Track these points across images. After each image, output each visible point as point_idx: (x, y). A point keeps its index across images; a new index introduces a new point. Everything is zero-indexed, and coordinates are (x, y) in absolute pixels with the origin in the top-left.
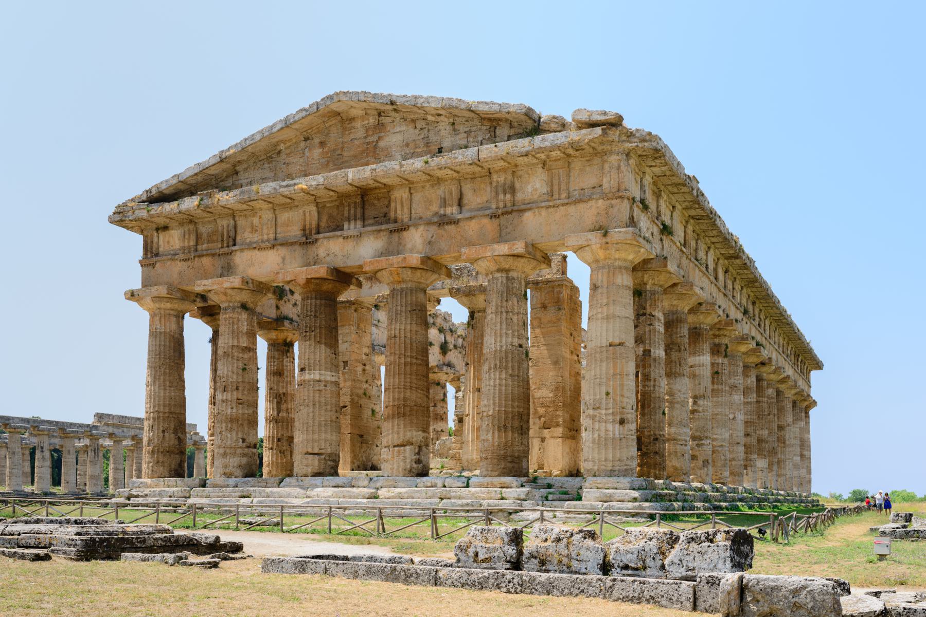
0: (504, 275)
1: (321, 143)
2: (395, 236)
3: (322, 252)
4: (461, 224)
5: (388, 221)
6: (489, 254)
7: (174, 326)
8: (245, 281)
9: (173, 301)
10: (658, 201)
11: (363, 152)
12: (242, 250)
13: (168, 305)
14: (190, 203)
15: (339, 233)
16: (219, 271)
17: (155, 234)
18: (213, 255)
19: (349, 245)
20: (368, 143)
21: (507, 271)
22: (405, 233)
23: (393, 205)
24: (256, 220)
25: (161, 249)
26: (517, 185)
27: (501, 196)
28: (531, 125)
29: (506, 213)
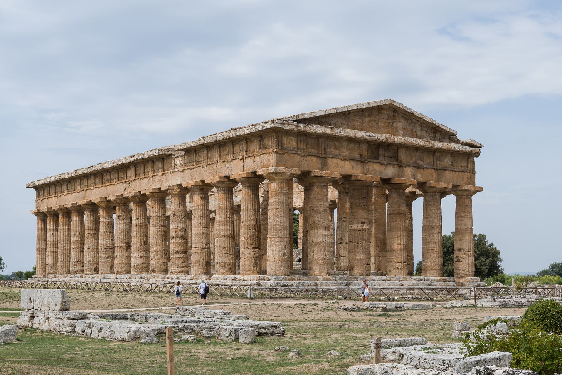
2: (401, 168)
3: (371, 169)
4: (425, 169)
5: (397, 161)
11: (387, 126)
12: (332, 158)
14: (320, 129)
16: (320, 166)
18: (317, 156)
19: (382, 168)
20: (389, 123)
22: (405, 168)
24: (337, 144)
27: (438, 162)
28: (450, 136)
29: (441, 169)
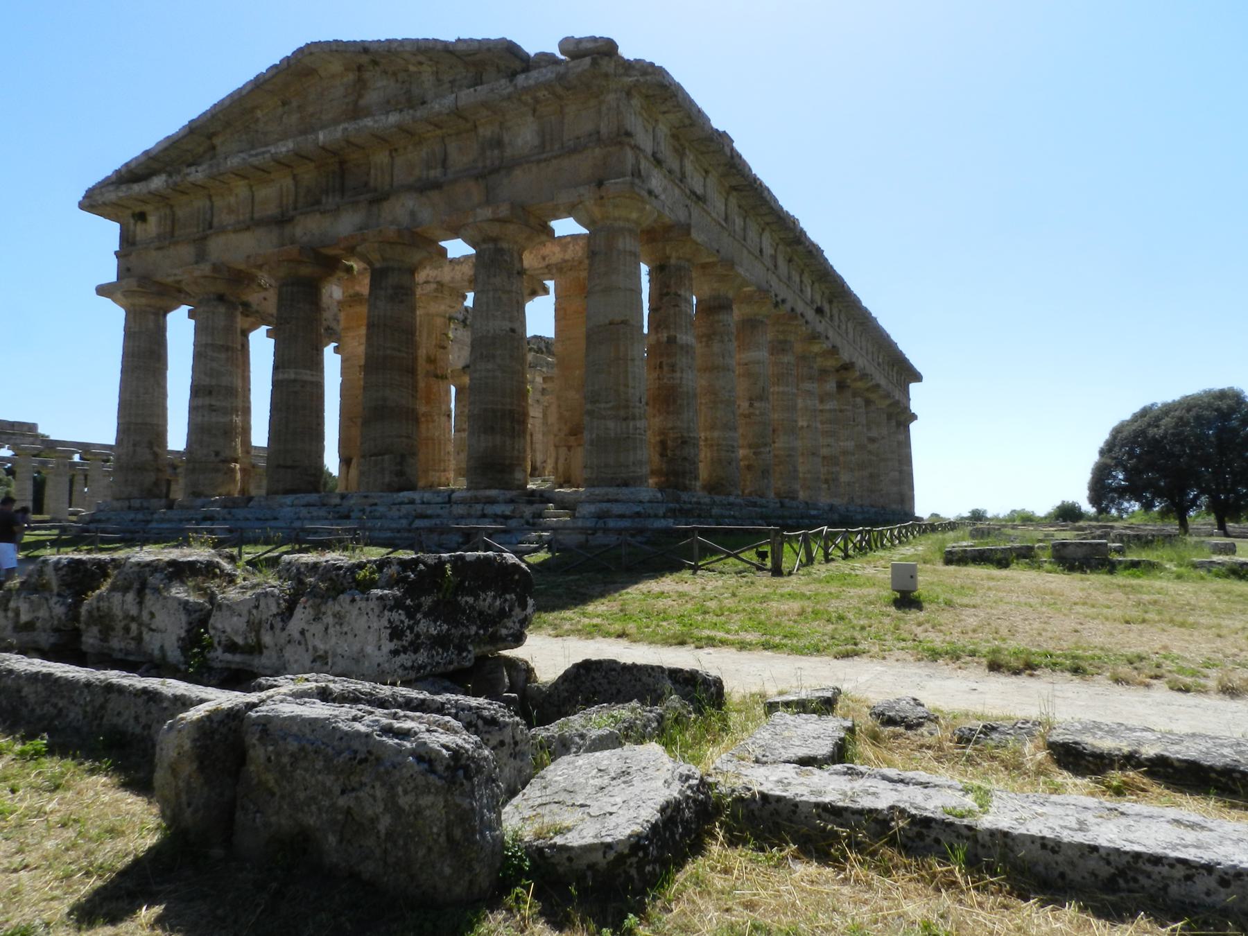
0: (491, 246)
1: (299, 107)
3: (299, 231)
6: (471, 220)
7: (151, 325)
8: (216, 268)
9: (142, 292)
10: (681, 161)
13: (143, 301)
15: (316, 207)
17: (132, 221)
21: (495, 240)
23: (373, 172)
25: (138, 238)
26: (506, 139)
